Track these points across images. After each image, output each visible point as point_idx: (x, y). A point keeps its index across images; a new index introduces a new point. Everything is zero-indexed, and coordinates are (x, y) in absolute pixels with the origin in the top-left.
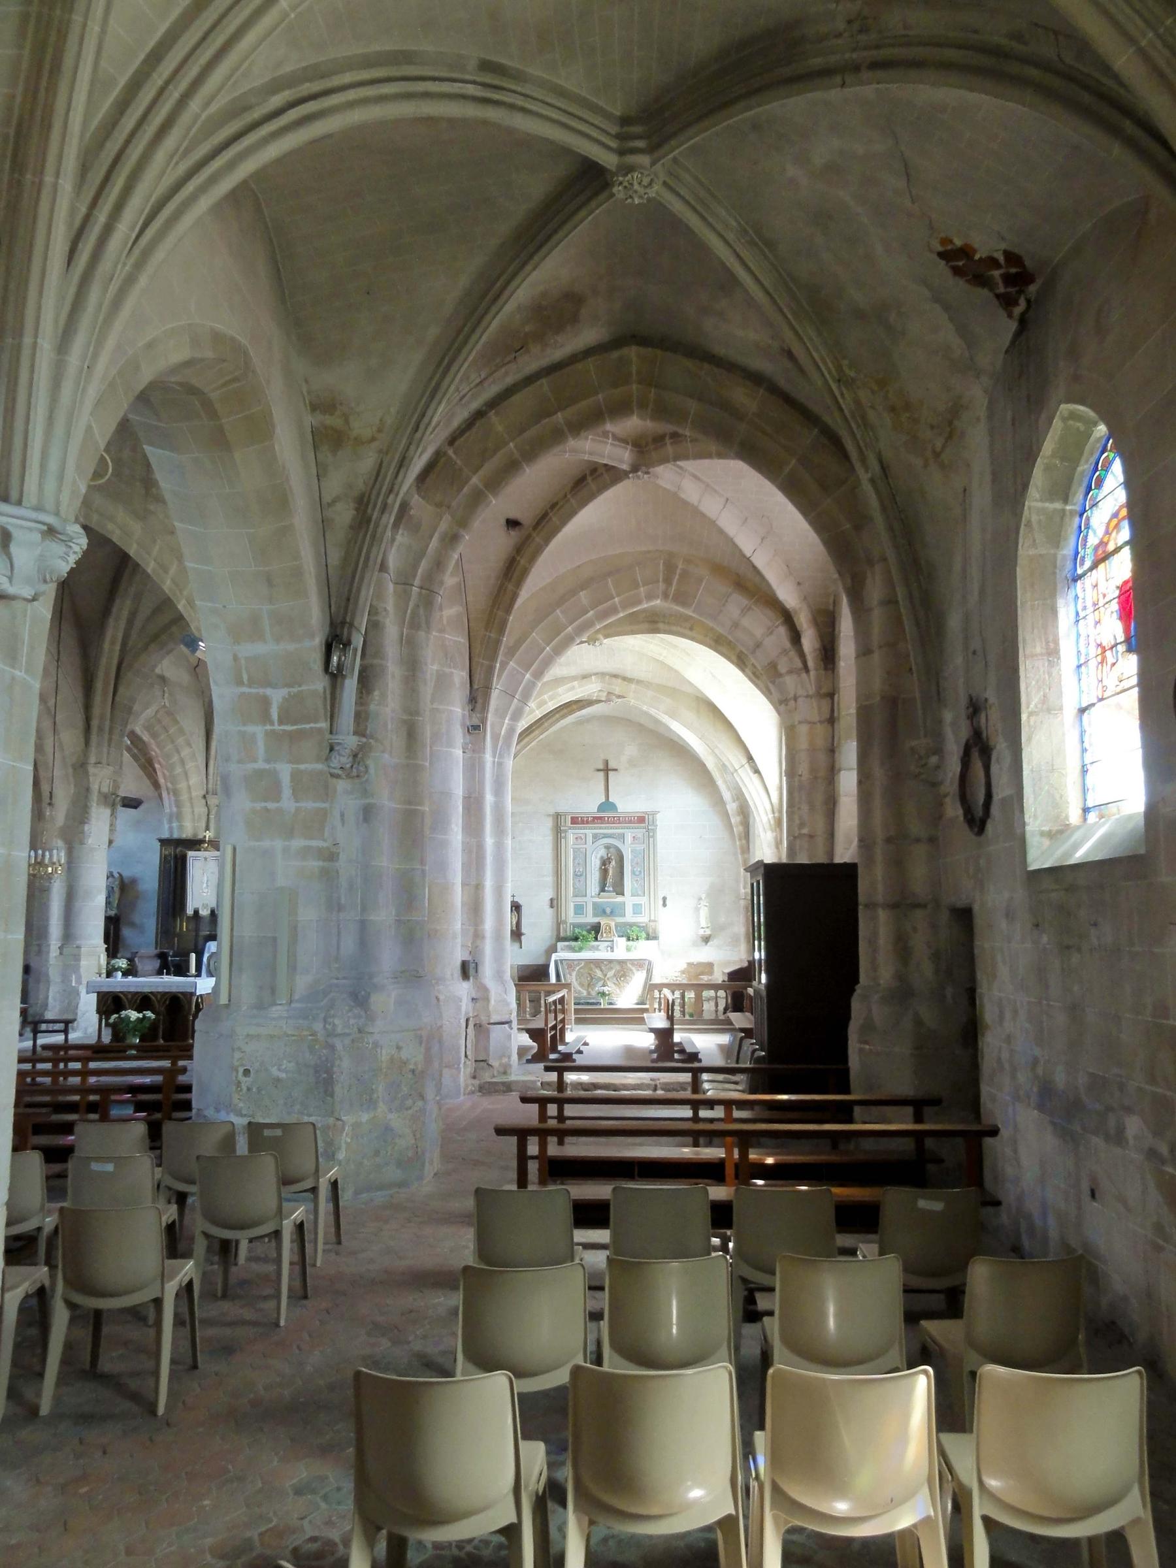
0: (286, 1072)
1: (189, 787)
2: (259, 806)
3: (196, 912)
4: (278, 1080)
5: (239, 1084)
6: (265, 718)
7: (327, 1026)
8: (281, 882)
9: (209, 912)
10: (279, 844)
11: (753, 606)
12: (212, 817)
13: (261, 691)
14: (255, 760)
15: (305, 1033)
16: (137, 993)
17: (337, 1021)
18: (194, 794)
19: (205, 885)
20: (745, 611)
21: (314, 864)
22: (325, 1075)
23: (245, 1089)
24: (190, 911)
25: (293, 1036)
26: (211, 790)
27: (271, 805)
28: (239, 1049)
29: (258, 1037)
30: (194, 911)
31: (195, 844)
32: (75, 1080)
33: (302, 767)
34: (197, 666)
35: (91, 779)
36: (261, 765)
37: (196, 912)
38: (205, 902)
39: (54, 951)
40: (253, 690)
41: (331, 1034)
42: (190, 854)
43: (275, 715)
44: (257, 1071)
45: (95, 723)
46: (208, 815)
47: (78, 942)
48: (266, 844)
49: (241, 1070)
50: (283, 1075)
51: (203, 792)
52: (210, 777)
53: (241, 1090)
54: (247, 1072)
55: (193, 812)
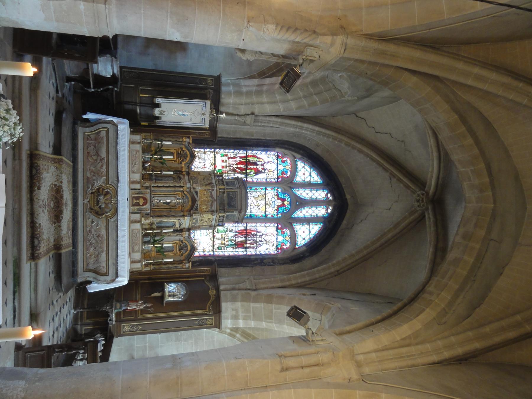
1: (262, 103)
3: (158, 106)
9: (157, 115)
12: (236, 118)
18: (256, 106)
24: (157, 101)
26: (258, 118)
30: (158, 104)
31: (216, 106)
34: (356, 116)
37: (158, 106)
38: (166, 113)
42: (209, 103)
45: (391, 48)
46: (238, 115)
51: (256, 113)
52: (268, 118)
55: (242, 104)
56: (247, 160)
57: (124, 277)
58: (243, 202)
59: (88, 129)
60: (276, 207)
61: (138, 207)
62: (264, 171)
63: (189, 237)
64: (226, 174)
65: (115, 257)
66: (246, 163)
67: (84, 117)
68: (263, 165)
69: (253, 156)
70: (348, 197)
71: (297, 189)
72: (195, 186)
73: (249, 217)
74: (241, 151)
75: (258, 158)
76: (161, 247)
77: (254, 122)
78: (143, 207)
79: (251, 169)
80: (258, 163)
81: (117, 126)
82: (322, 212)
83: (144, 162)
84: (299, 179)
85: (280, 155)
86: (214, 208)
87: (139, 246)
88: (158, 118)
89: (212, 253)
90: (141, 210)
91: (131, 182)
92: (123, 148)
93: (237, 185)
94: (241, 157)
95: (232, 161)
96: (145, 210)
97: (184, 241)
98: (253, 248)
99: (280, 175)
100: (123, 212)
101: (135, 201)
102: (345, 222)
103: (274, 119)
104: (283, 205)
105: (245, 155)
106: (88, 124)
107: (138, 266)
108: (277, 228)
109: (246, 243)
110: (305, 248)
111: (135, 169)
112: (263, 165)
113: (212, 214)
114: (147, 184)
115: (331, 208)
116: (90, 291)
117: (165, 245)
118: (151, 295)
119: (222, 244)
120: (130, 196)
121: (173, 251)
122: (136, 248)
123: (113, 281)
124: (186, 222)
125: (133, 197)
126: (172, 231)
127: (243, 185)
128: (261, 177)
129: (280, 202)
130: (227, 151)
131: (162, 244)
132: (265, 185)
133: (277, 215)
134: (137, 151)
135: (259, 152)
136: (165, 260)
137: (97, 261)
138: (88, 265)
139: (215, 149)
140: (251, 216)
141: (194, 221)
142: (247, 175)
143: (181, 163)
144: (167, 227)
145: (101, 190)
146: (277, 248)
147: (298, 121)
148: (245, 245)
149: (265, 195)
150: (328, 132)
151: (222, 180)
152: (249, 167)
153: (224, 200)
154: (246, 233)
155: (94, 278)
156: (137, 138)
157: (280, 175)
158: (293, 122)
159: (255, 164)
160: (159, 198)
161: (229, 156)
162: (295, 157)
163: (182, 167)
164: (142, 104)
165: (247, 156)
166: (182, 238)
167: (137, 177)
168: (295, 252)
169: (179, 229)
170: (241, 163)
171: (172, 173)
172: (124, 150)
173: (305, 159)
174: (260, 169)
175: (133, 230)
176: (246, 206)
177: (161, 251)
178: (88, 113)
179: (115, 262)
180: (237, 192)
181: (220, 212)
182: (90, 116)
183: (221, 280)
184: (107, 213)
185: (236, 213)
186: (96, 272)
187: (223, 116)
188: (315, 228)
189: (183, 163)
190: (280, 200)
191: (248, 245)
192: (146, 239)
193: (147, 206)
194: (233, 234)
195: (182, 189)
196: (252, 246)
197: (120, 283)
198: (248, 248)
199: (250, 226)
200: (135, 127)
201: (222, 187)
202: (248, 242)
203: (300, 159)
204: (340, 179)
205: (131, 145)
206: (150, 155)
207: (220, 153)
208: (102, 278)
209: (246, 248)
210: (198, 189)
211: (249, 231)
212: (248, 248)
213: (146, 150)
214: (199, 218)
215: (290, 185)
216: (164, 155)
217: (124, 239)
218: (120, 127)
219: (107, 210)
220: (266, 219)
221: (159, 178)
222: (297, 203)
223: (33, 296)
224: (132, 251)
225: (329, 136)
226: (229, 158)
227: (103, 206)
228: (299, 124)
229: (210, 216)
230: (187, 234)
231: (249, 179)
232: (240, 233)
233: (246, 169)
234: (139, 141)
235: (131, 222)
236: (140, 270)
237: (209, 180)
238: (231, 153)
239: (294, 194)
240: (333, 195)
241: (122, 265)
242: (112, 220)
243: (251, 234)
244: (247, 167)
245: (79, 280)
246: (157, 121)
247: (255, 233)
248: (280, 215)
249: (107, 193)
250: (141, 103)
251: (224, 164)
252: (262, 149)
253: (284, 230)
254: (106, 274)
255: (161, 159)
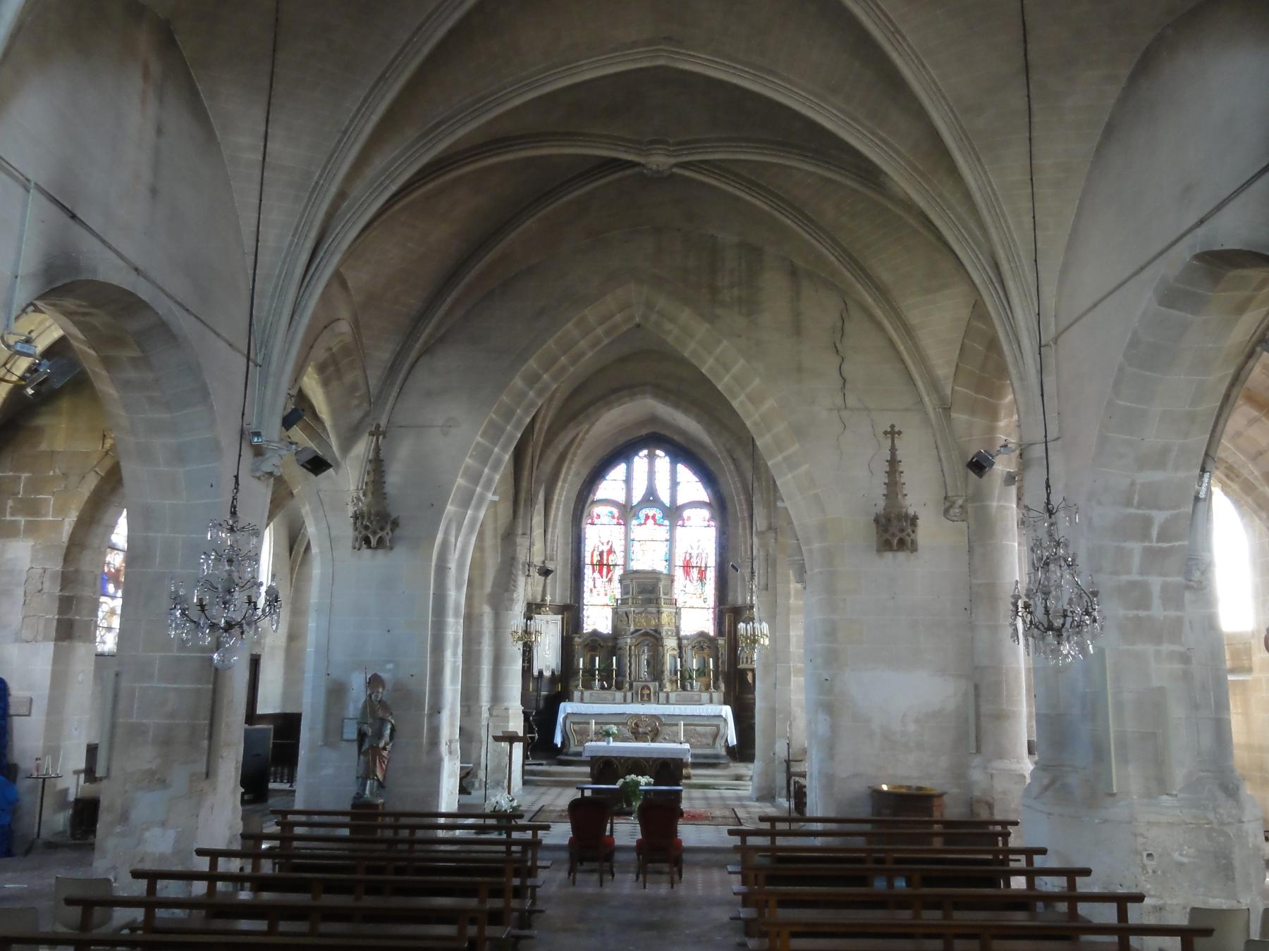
0: (1187, 856)
2: (1131, 613)
3: (541, 673)
4: (1181, 864)
5: (1144, 867)
6: (1145, 536)
7: (1218, 816)
8: (1156, 682)
10: (1150, 648)
11: (1263, 419)
13: (1147, 512)
14: (1128, 572)
15: (1202, 822)
16: (629, 758)
17: (1222, 811)
19: (547, 647)
20: (1252, 422)
21: (1177, 666)
22: (1224, 861)
23: (1150, 871)
24: (536, 673)
25: (1191, 823)
26: (548, 556)
27: (1142, 613)
28: (1142, 835)
29: (1158, 824)
30: (539, 673)
32: (389, 834)
33: (1169, 579)
35: (518, 548)
36: (1135, 577)
37: (541, 673)
39: (485, 714)
40: (1140, 512)
41: (1222, 823)
43: (1154, 533)
44: (1160, 856)
47: (506, 704)
48: (1139, 647)
49: (1145, 854)
50: (1185, 860)
51: (543, 559)
52: (549, 544)
53: (1147, 873)
54: (1149, 855)
56: (597, 565)
57: (721, 710)
58: (649, 576)
59: (572, 742)
60: (656, 526)
61: (652, 695)
62: (610, 544)
63: (687, 638)
64: (614, 590)
65: (701, 718)
66: (599, 565)
67: (559, 746)
68: (603, 544)
69: (592, 556)
70: (644, 432)
71: (633, 498)
72: (628, 633)
73: (667, 563)
74: (586, 571)
75: (594, 550)
76: (697, 671)
77: (553, 560)
78: (652, 690)
79: (608, 560)
80: (600, 550)
81: (568, 714)
82: (663, 461)
83: (602, 688)
84: (621, 498)
85: (590, 521)
86: (654, 610)
87: (695, 694)
88: (553, 673)
89: (712, 610)
90: (655, 692)
91: (625, 701)
92: (591, 709)
93: (628, 582)
94: (594, 571)
95: (599, 582)
96: (655, 688)
97: (693, 645)
98: (706, 558)
99: (615, 521)
100: (655, 709)
101: (645, 698)
102: (676, 438)
103: (549, 536)
104: (654, 517)
105: (591, 566)
106: (566, 742)
107: (717, 696)
108: (683, 526)
109: (701, 567)
110: (709, 490)
111: (610, 697)
112: (603, 544)
113: (662, 613)
114: (627, 686)
115: (658, 452)
116: (735, 743)
117: (694, 667)
118: (750, 684)
119: (701, 597)
120: (639, 703)
121: (704, 658)
122: (696, 698)
123: (725, 720)
124: (670, 643)
125: (641, 700)
126: (679, 659)
127: (629, 576)
128: (619, 547)
129: (650, 521)
130: (585, 589)
131: (694, 670)
132: (628, 541)
133: (666, 526)
134: (591, 695)
135: (587, 548)
136: (711, 667)
137: (704, 735)
138: (708, 744)
139: (584, 605)
140: (666, 561)
141: (669, 633)
142: (616, 565)
143: (602, 647)
144: (676, 662)
145: (634, 731)
146: (709, 526)
147: (551, 506)
148: (703, 569)
149: (642, 542)
150: (564, 470)
151: (622, 600)
152: (605, 562)
153: (647, 599)
154: (687, 567)
155: (722, 738)
156: (577, 694)
157: (615, 521)
158: (553, 513)
159: (601, 554)
160: (643, 672)
161: (592, 586)
162: (593, 502)
163: (608, 646)
164: (538, 690)
165: (593, 565)
166: (690, 647)
167: (619, 695)
168: (714, 504)
169: (678, 651)
170: (600, 572)
171: (614, 658)
172: (592, 707)
173: (595, 487)
174: (608, 547)
175: (676, 701)
176: (654, 572)
177: (702, 672)
178: (555, 742)
179: (706, 719)
180: (636, 582)
181: (661, 604)
182: (558, 740)
183: (740, 602)
184: (656, 725)
185: (661, 585)
186: (716, 736)
187: (548, 598)
188: (684, 472)
189: (602, 644)
190: (647, 522)
191: (703, 565)
192: (689, 688)
193: (651, 685)
194: (688, 582)
195: (633, 647)
196: (704, 560)
197: (728, 714)
198: (706, 564)
199: (679, 561)
200: (566, 696)
201: (630, 601)
202: (699, 565)
203: (594, 495)
204: (621, 443)
205: (585, 701)
206: (593, 682)
207: (587, 598)
208: (722, 731)
209: (706, 567)
210: (632, 628)
211: (685, 563)
212: (706, 564)
213: (588, 686)
214: (665, 628)
215: (629, 510)
216: (595, 666)
217: (683, 710)
218: (569, 710)
219: (654, 724)
220: (671, 541)
221: (620, 672)
222: (651, 498)
223: (721, 778)
224: (699, 702)
225: (569, 468)
226: (595, 587)
227: (650, 729)
228: (554, 506)
229: (664, 615)
230: (685, 642)
231: (620, 561)
232: (687, 573)
233: (608, 566)
234: (580, 693)
235: (668, 702)
236: (722, 694)
237: (622, 616)
238: (588, 584)
239: (639, 503)
240: (641, 449)
241: (709, 711)
242: (663, 720)
243: (690, 558)
244: (606, 565)
245: (723, 752)
246: (556, 673)
247: (688, 555)
248: (667, 522)
249: (636, 724)
250: (537, 691)
251: (602, 593)
252: (583, 545)
253: (686, 518)
254: (718, 727)
255: (598, 670)
